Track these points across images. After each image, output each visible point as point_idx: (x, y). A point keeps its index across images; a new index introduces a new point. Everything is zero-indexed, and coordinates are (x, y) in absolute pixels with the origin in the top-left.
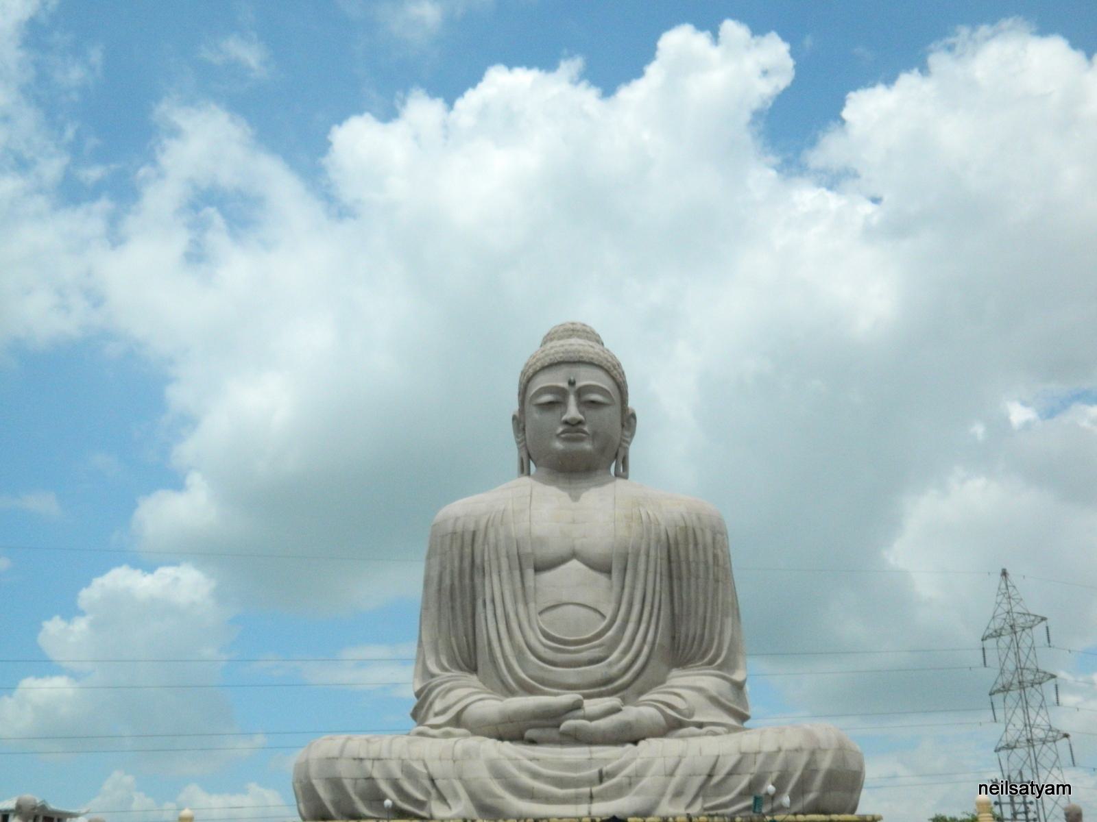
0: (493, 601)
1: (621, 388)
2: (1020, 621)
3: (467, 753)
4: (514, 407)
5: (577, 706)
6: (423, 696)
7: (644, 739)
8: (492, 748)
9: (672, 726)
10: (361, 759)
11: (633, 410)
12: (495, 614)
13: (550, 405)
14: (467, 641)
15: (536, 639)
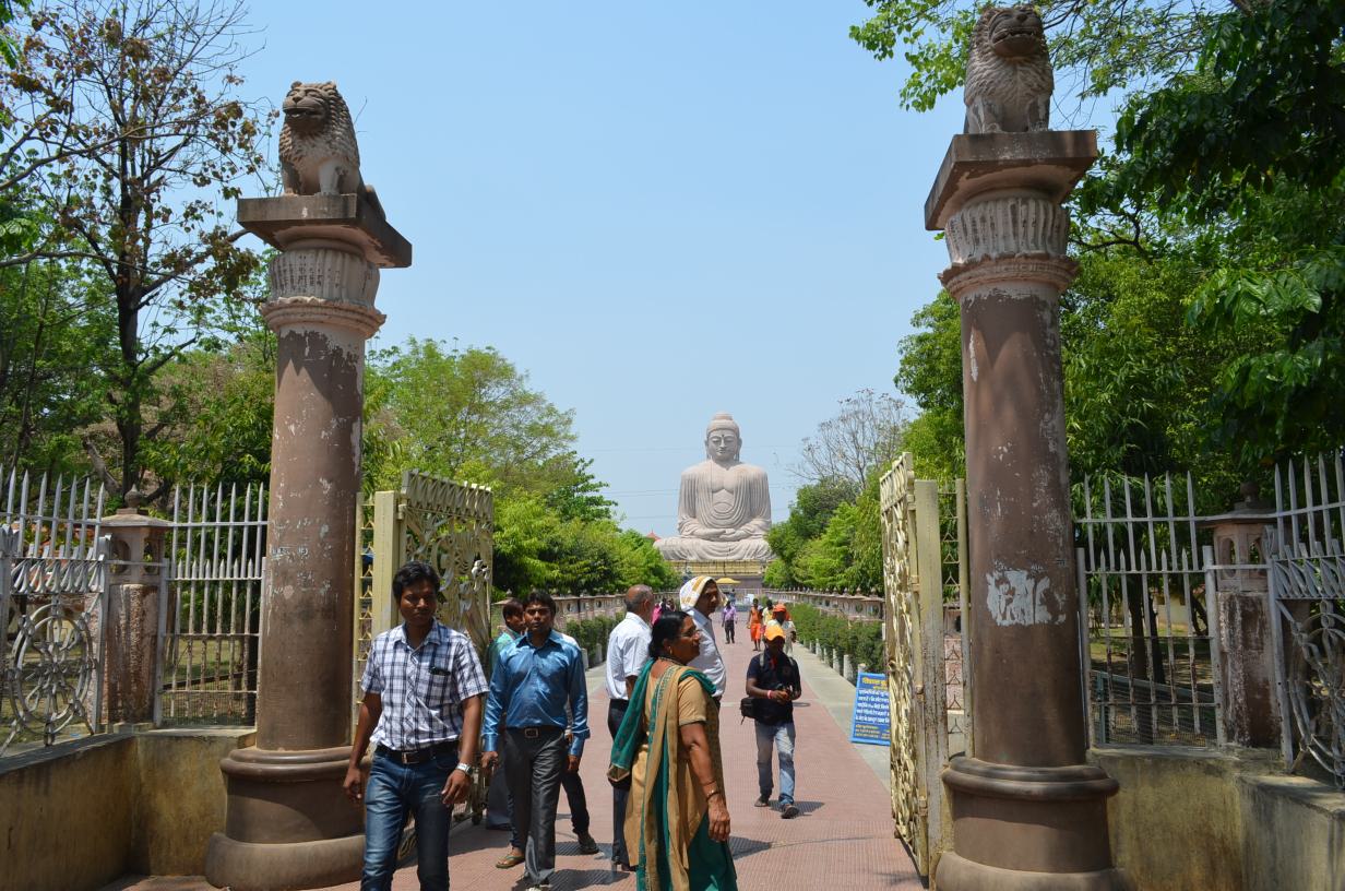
1: (737, 434)
3: (698, 544)
6: (681, 525)
9: (748, 536)
15: (714, 514)
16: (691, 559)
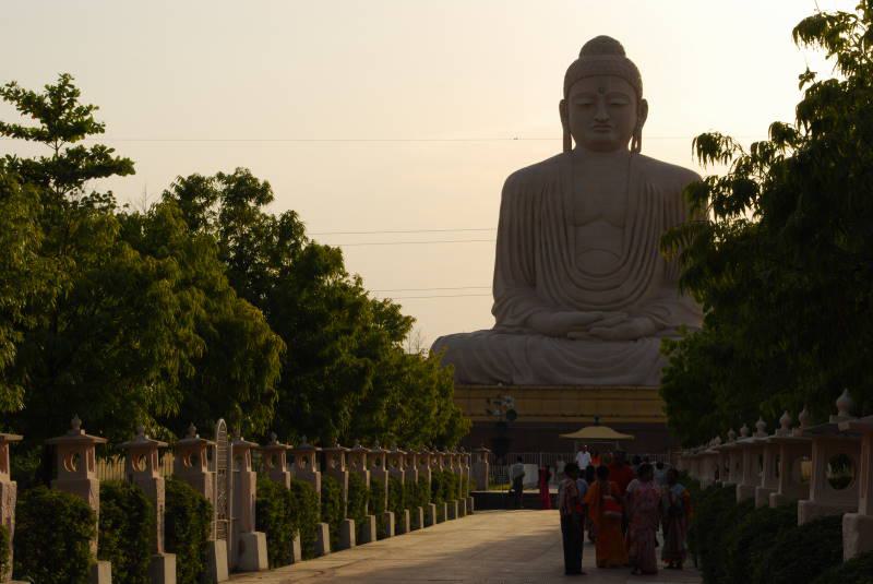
0: (546, 244)
4: (562, 98)
11: (645, 101)
12: (547, 254)
13: (587, 105)
14: (529, 269)
16: (517, 380)
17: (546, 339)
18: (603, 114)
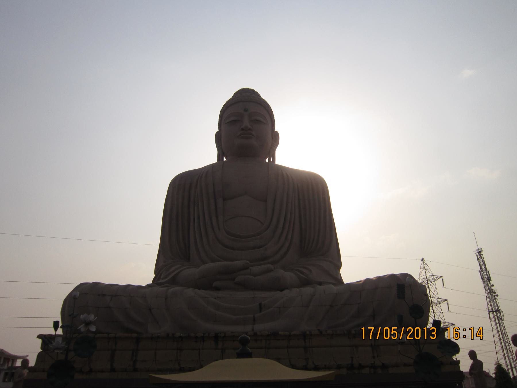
0: (199, 218)
2: (430, 279)
5: (245, 268)
7: (287, 289)
8: (190, 292)
9: (306, 283)
10: (103, 295)
11: (277, 132)
12: (199, 225)
17: (191, 289)
18: (246, 123)
